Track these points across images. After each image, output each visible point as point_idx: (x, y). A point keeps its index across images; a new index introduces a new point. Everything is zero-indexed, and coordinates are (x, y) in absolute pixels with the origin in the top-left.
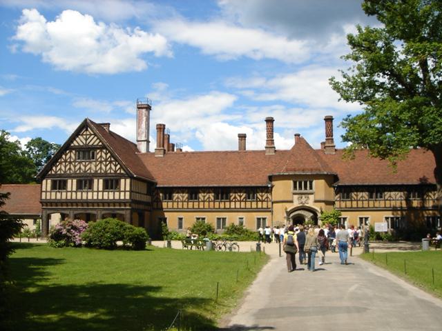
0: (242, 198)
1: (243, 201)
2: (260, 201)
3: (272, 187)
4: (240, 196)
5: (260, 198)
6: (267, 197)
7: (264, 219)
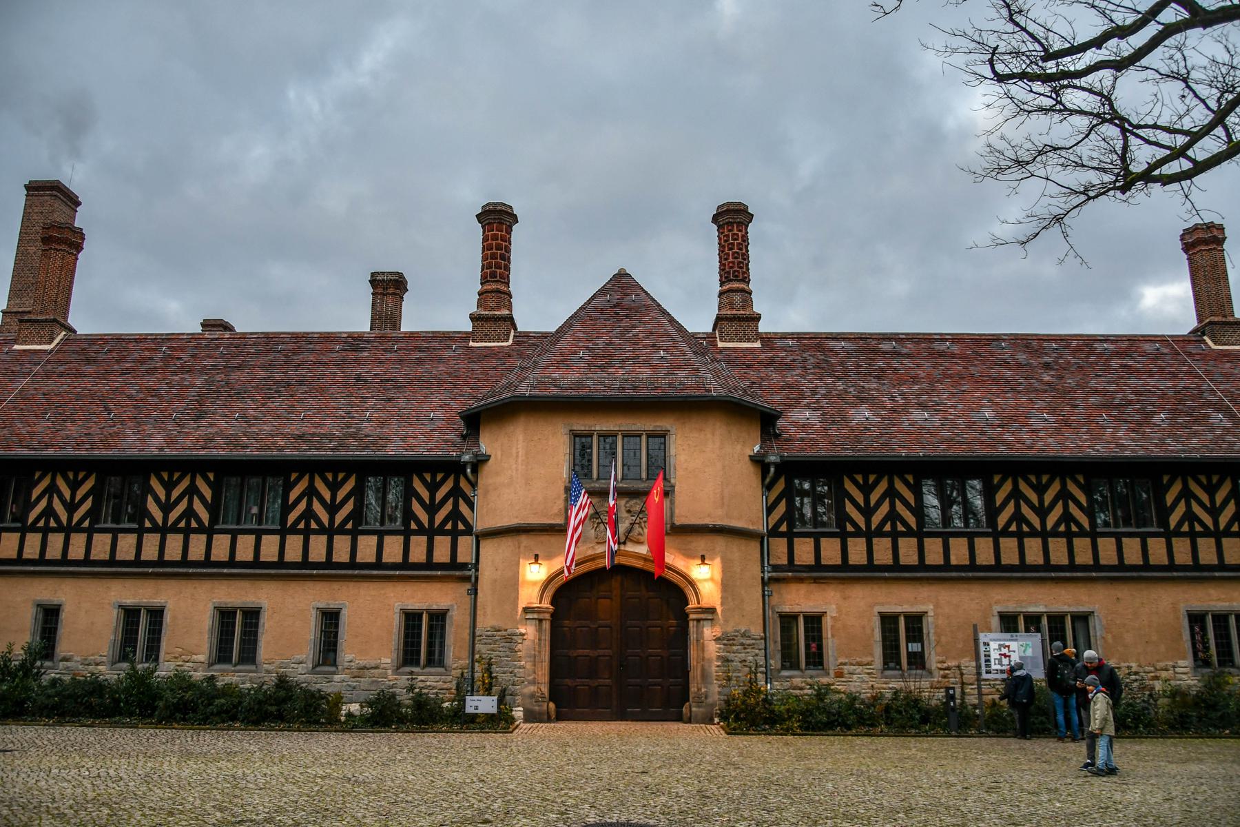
0: (339, 518)
1: (341, 530)
2: (421, 531)
3: (480, 462)
4: (333, 509)
6: (455, 515)
7: (439, 618)
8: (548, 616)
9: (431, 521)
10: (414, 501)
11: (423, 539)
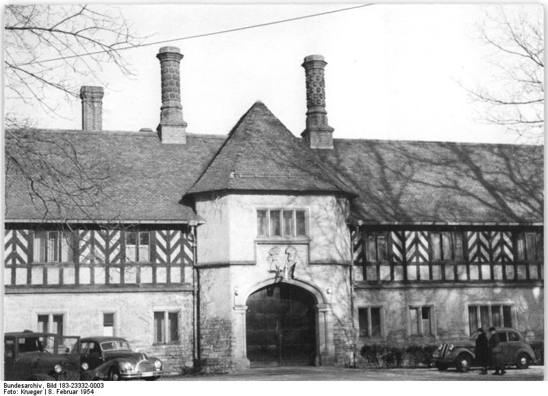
2: (163, 264)
5: (164, 257)
6: (182, 255)
8: (245, 311)
9: (169, 259)
10: (157, 247)
11: (164, 269)
